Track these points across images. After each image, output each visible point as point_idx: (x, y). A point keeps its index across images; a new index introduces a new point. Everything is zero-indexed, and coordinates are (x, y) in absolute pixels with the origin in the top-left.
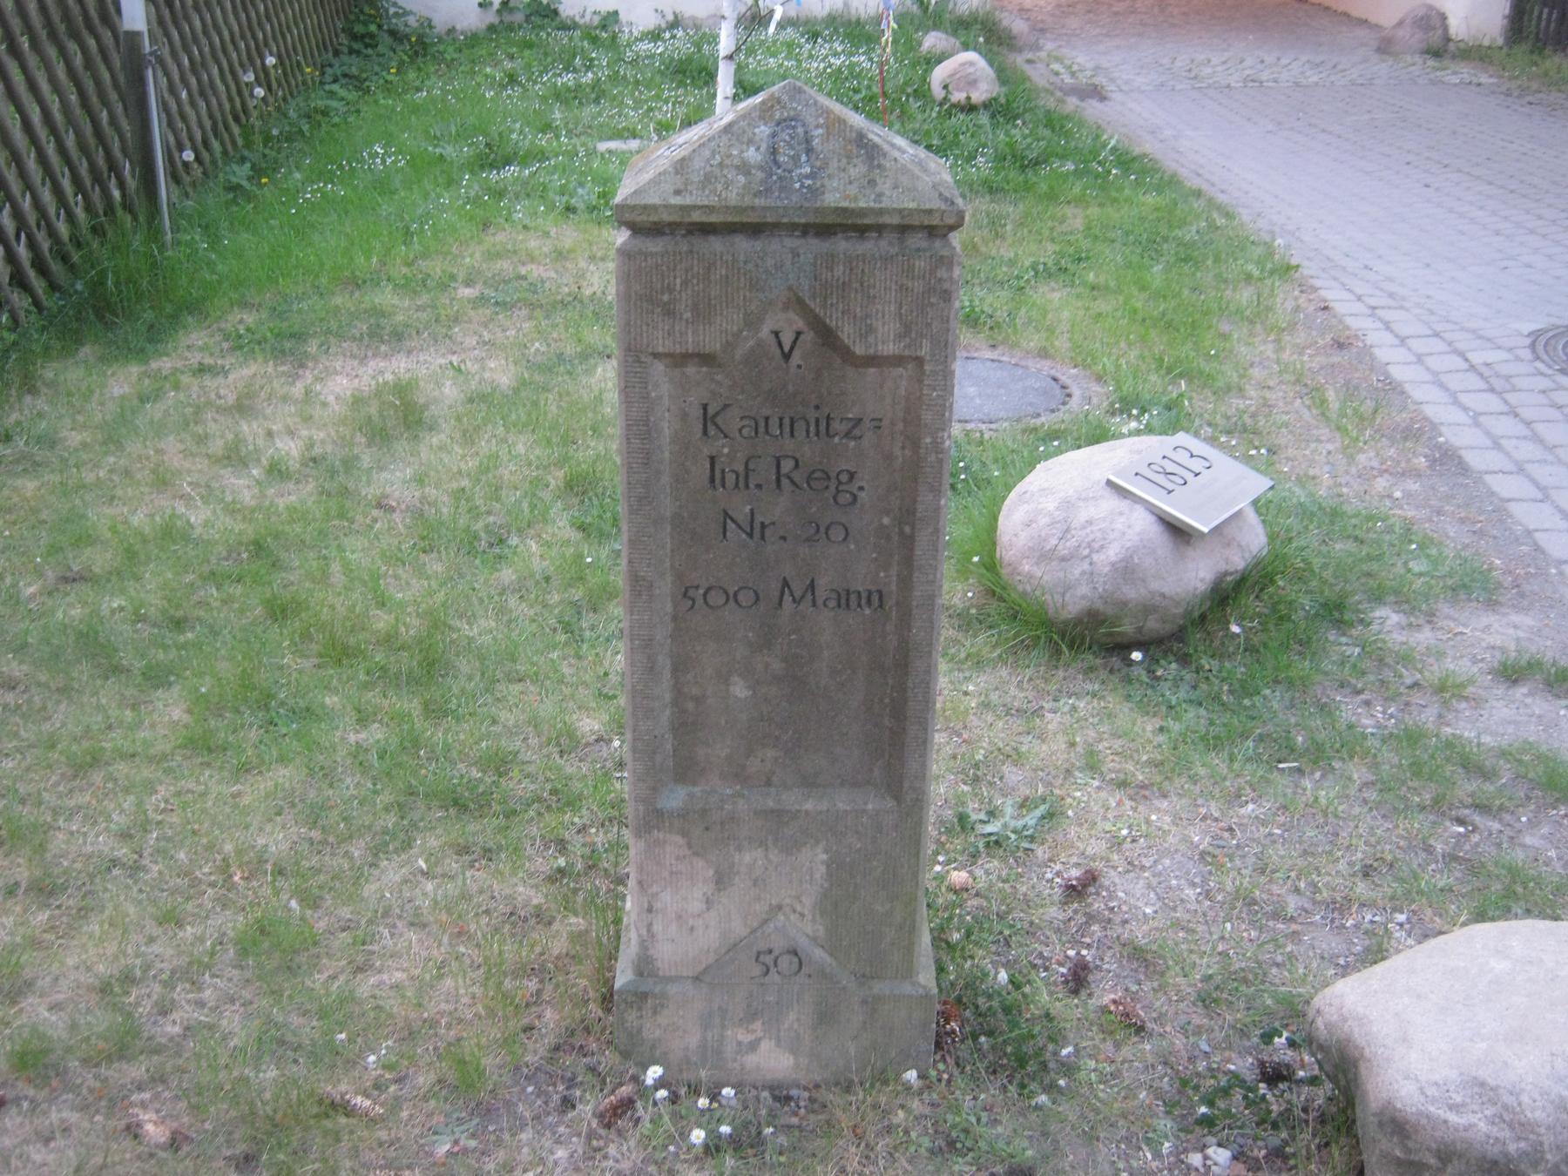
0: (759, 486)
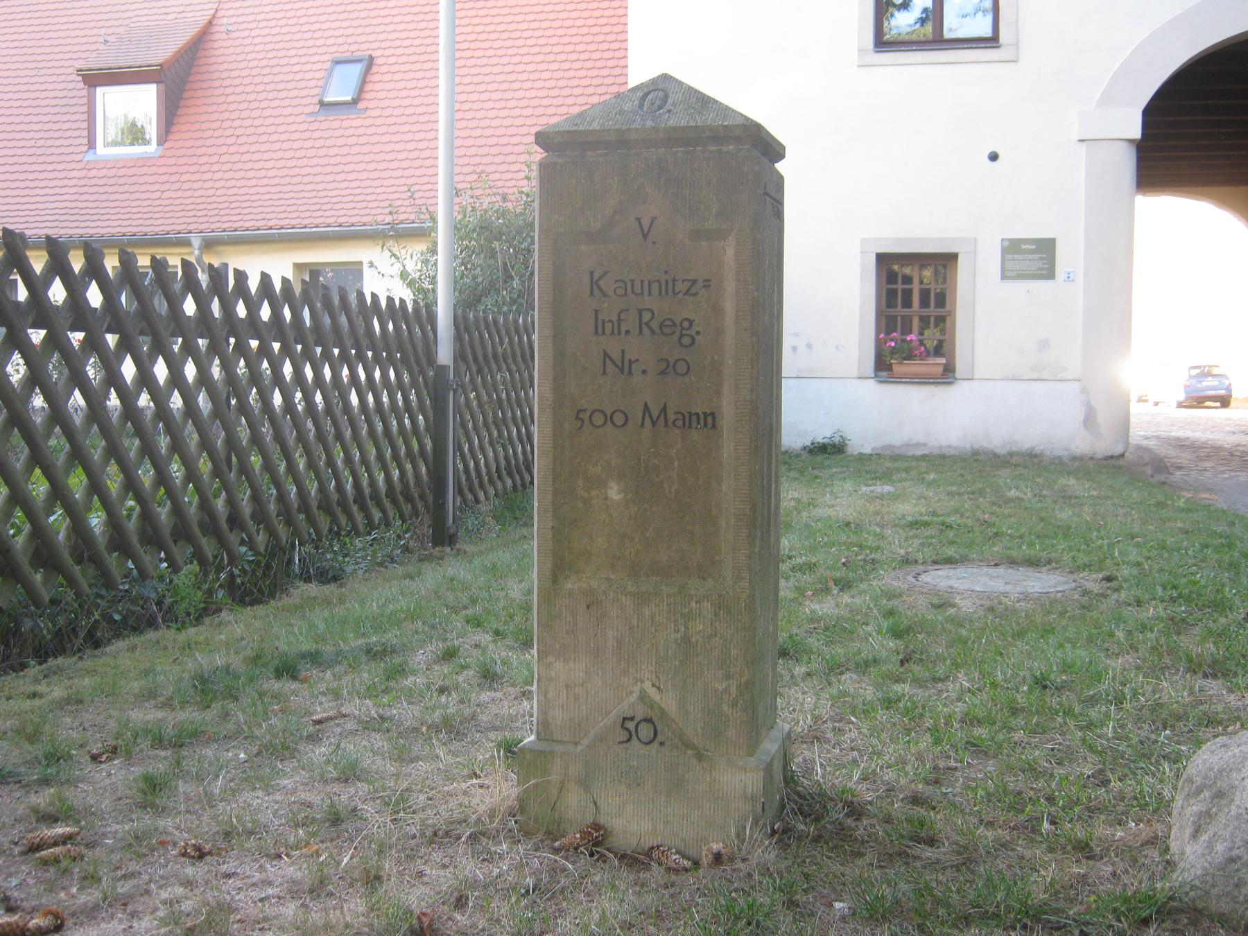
0: (627, 332)
